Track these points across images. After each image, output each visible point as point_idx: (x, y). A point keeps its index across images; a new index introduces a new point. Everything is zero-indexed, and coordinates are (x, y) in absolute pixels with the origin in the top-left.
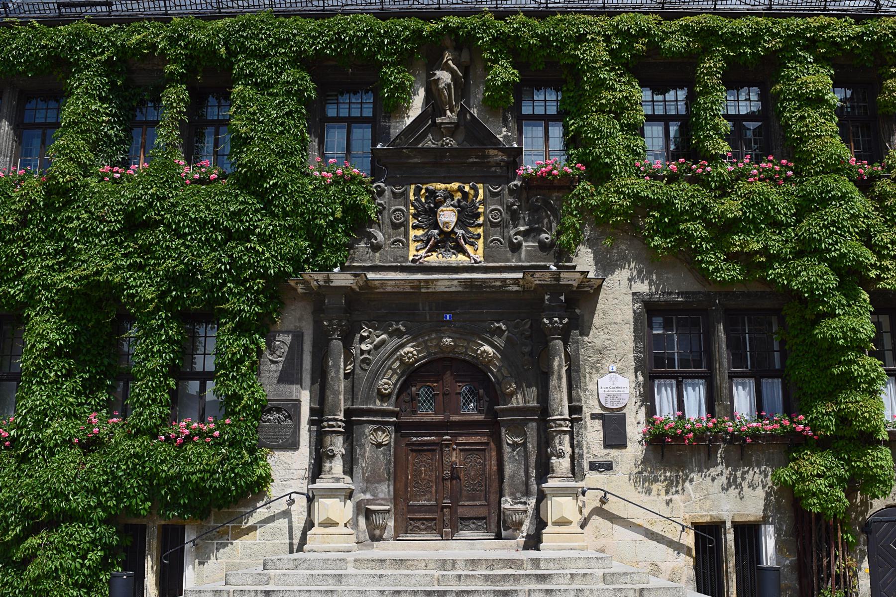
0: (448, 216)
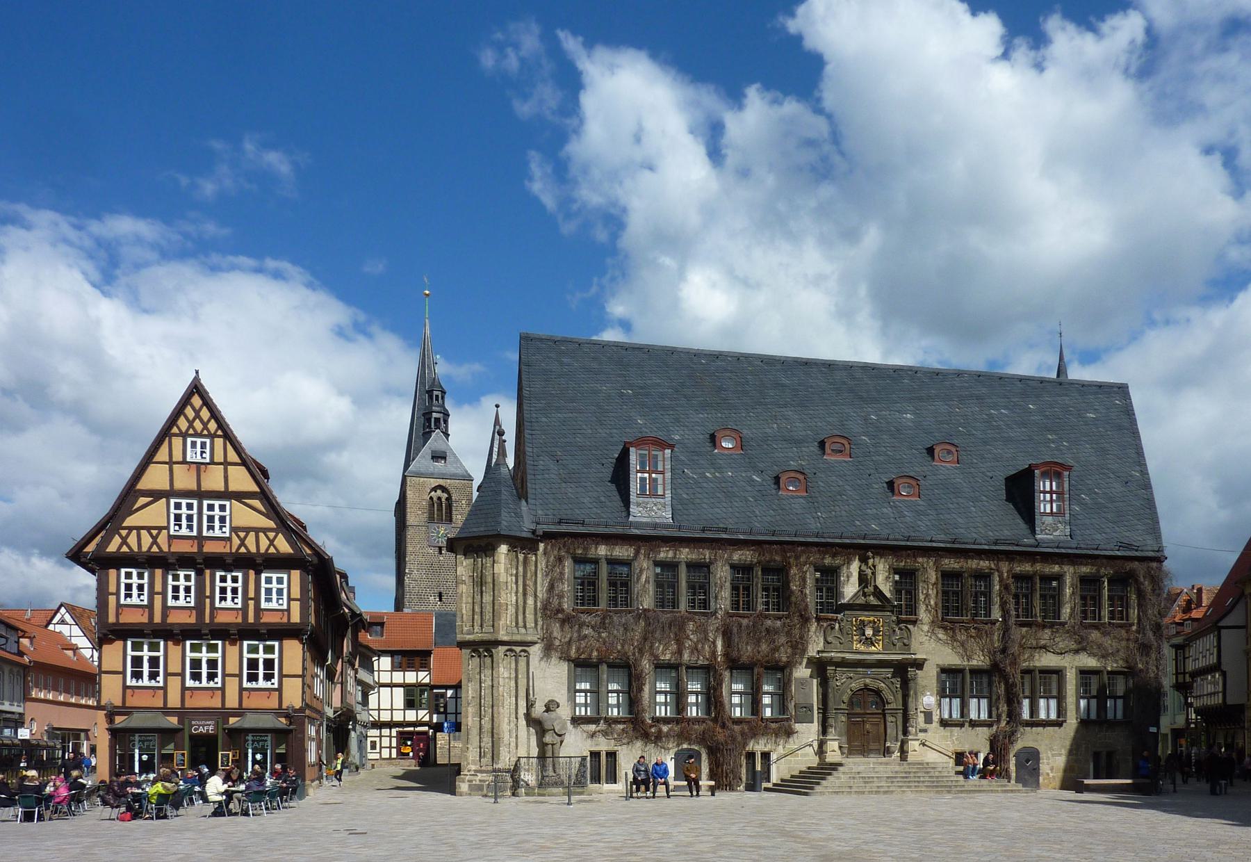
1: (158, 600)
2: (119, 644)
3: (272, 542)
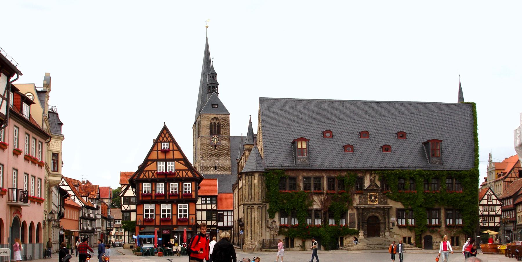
0: (373, 198)
1: (154, 192)
2: (142, 205)
3: (187, 174)
